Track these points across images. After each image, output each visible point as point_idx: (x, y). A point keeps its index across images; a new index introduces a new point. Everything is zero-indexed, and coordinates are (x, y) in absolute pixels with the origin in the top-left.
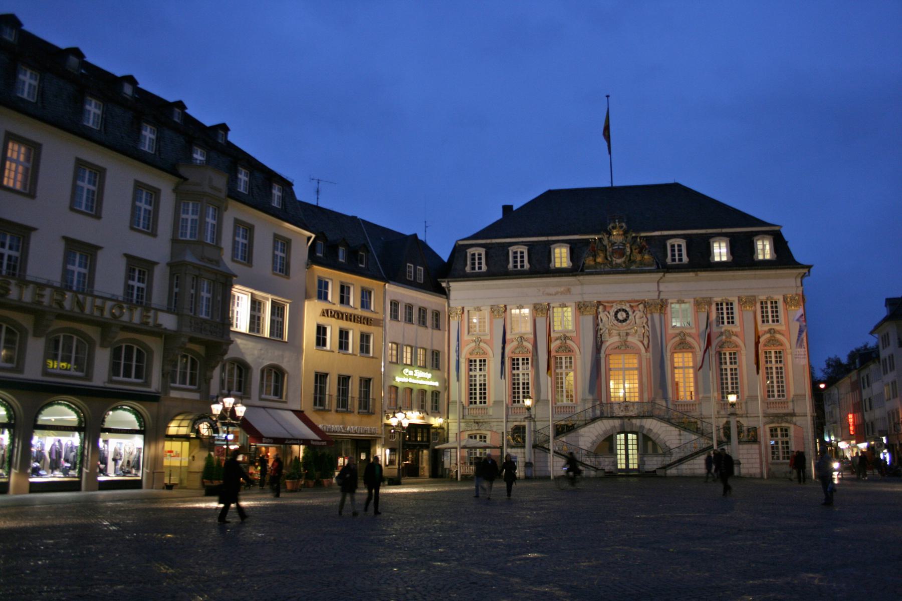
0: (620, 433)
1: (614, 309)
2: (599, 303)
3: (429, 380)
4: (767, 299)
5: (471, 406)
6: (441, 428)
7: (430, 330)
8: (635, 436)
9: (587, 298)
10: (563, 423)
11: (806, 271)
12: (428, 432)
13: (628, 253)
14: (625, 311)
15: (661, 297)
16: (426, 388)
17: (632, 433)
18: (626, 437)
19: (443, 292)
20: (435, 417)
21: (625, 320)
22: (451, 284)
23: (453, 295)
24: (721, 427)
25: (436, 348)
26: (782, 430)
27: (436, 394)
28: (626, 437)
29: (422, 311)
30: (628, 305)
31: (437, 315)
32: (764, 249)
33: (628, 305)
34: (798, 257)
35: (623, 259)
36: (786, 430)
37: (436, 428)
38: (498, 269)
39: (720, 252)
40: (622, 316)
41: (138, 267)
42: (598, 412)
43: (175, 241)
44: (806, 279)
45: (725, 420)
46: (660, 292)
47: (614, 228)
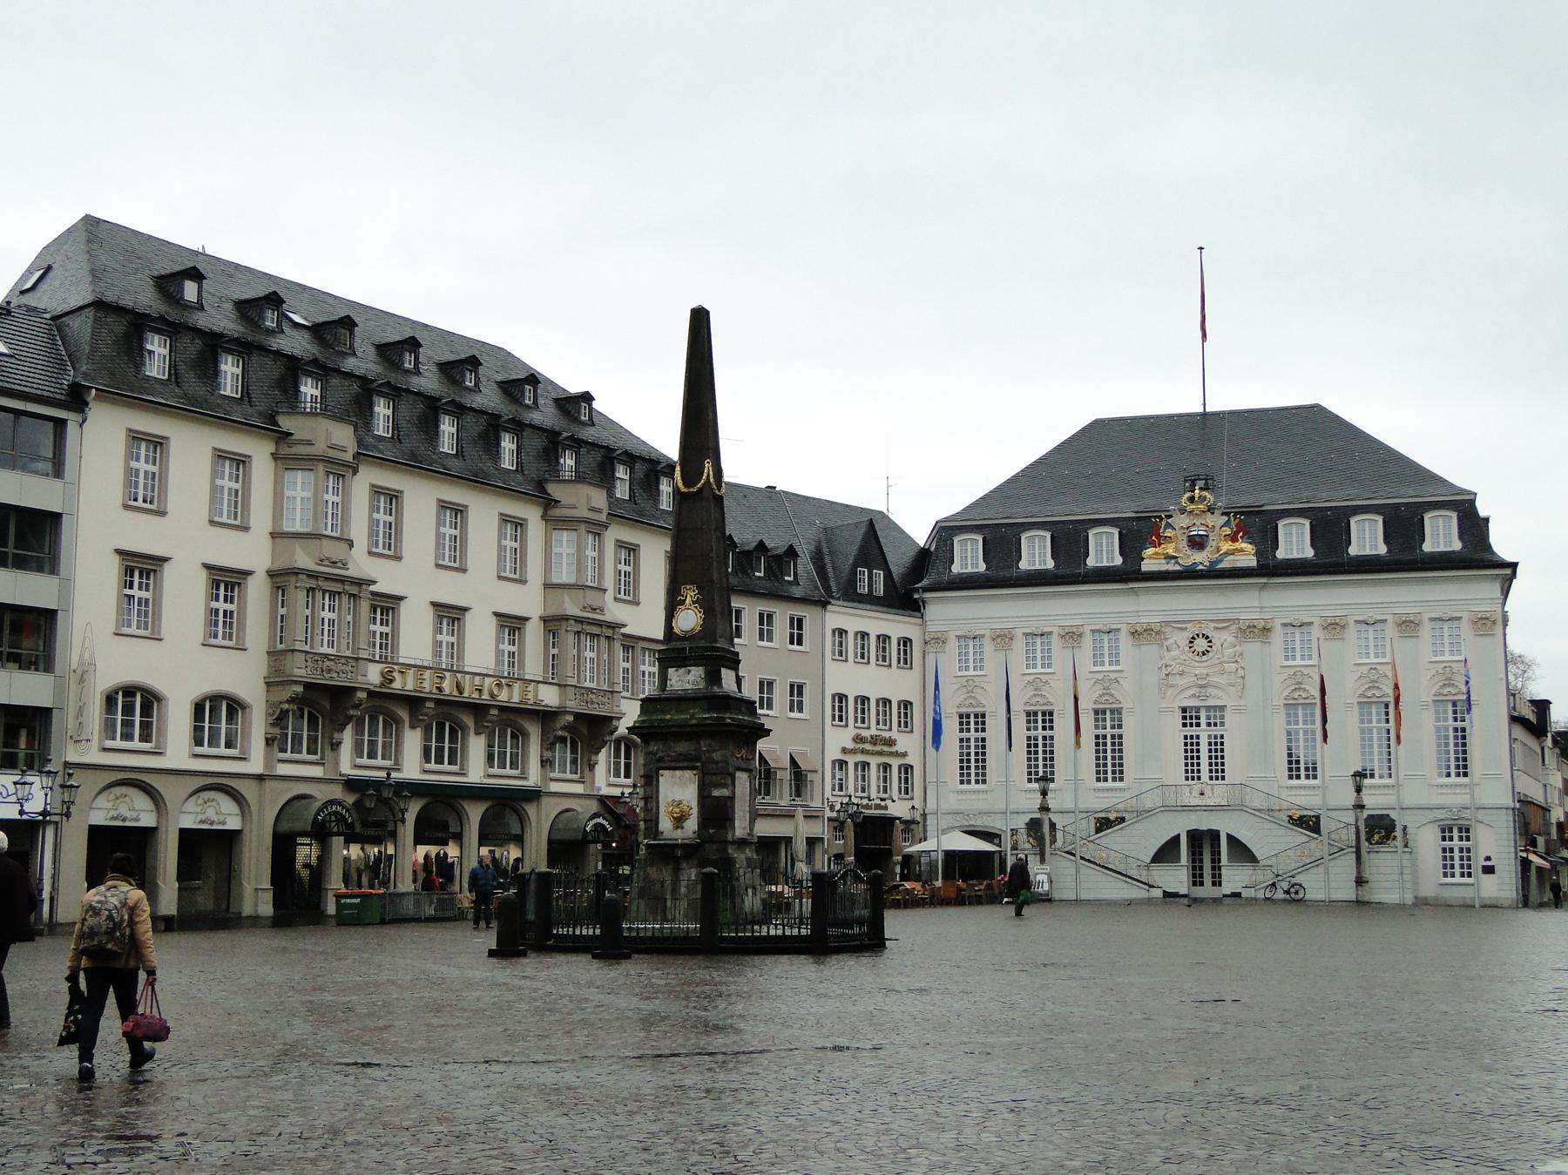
1: (1187, 635)
26: (1460, 830)
29: (883, 639)
30: (1212, 625)
31: (906, 642)
32: (1441, 535)
36: (1468, 831)
39: (1367, 538)
40: (1201, 644)
41: (511, 624)
43: (548, 586)
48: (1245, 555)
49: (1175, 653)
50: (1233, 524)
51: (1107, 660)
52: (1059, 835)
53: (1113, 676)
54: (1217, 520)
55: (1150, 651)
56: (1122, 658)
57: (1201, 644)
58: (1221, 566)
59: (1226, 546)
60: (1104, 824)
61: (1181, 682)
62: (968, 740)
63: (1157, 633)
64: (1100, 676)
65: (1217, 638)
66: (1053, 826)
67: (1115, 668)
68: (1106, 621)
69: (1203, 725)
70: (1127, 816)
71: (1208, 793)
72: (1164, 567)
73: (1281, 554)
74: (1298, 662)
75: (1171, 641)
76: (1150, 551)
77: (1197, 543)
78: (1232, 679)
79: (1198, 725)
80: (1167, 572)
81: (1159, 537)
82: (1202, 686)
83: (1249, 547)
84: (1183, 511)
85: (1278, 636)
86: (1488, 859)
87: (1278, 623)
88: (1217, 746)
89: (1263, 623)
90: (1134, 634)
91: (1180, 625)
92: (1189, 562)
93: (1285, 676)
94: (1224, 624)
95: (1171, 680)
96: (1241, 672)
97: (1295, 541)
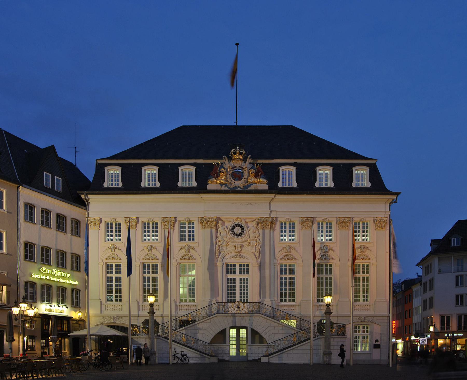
0: (232, 328)
3: (69, 279)
4: (361, 220)
5: (108, 303)
6: (80, 320)
7: (69, 235)
8: (245, 331)
9: (209, 214)
10: (184, 318)
11: (394, 197)
12: (69, 324)
13: (246, 177)
16: (65, 286)
17: (243, 327)
18: (238, 333)
19: (84, 204)
20: (76, 311)
21: (240, 234)
22: (90, 196)
23: (92, 206)
24: (316, 324)
25: (75, 251)
27: (76, 292)
28: (238, 333)
33: (243, 221)
34: (389, 186)
35: (241, 182)
37: (76, 320)
38: (131, 184)
40: (238, 230)
42: (214, 311)
44: (393, 205)
45: (318, 319)
46: (271, 212)
47: (235, 153)
48: (263, 184)
52: (160, 327)
58: (250, 188)
60: (184, 323)
62: (116, 273)
66: (156, 324)
69: (238, 273)
70: (197, 319)
71: (242, 307)
77: (237, 176)
79: (235, 273)
81: (217, 173)
86: (377, 341)
88: (244, 282)
92: (233, 186)
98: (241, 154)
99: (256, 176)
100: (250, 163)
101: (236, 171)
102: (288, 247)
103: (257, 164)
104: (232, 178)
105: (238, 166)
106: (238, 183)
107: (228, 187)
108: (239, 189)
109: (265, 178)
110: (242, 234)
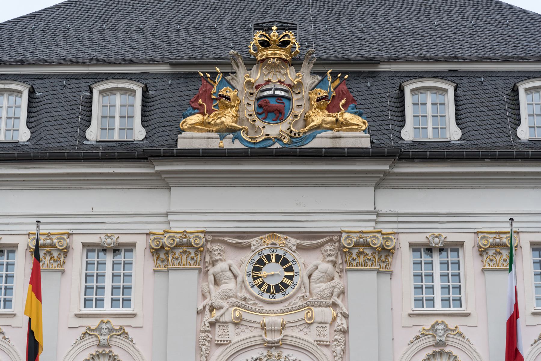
2: (217, 236)
14: (285, 262)
15: (387, 228)
30: (293, 242)
35: (283, 127)
40: (273, 272)
47: (265, 44)
49: (229, 286)
50: (332, 86)
51: (107, 296)
53: (116, 323)
54: (309, 81)
55: (185, 283)
56: (135, 295)
57: (273, 272)
59: (319, 117)
61: (234, 335)
63: (199, 250)
64: (94, 323)
65: (304, 262)
67: (120, 310)
68: (110, 228)
72: (216, 144)
73: (408, 134)
74: (438, 307)
75: (221, 266)
76: (196, 118)
77: (272, 109)
78: (328, 335)
80: (221, 149)
82: (271, 346)
83: (357, 120)
84: (251, 63)
85: (404, 262)
87: (404, 241)
89: (378, 242)
90: (158, 251)
91: (240, 240)
93: (416, 332)
94: (311, 240)
95: (218, 334)
96: (341, 322)
97: (431, 114)
98: (285, 44)
99: (332, 108)
100: (313, 73)
101: (270, 93)
102: (441, 327)
103: (334, 75)
104: (258, 114)
105: (275, 80)
106: (274, 130)
107: (242, 140)
108: (277, 145)
109: (360, 115)
110: (286, 286)
